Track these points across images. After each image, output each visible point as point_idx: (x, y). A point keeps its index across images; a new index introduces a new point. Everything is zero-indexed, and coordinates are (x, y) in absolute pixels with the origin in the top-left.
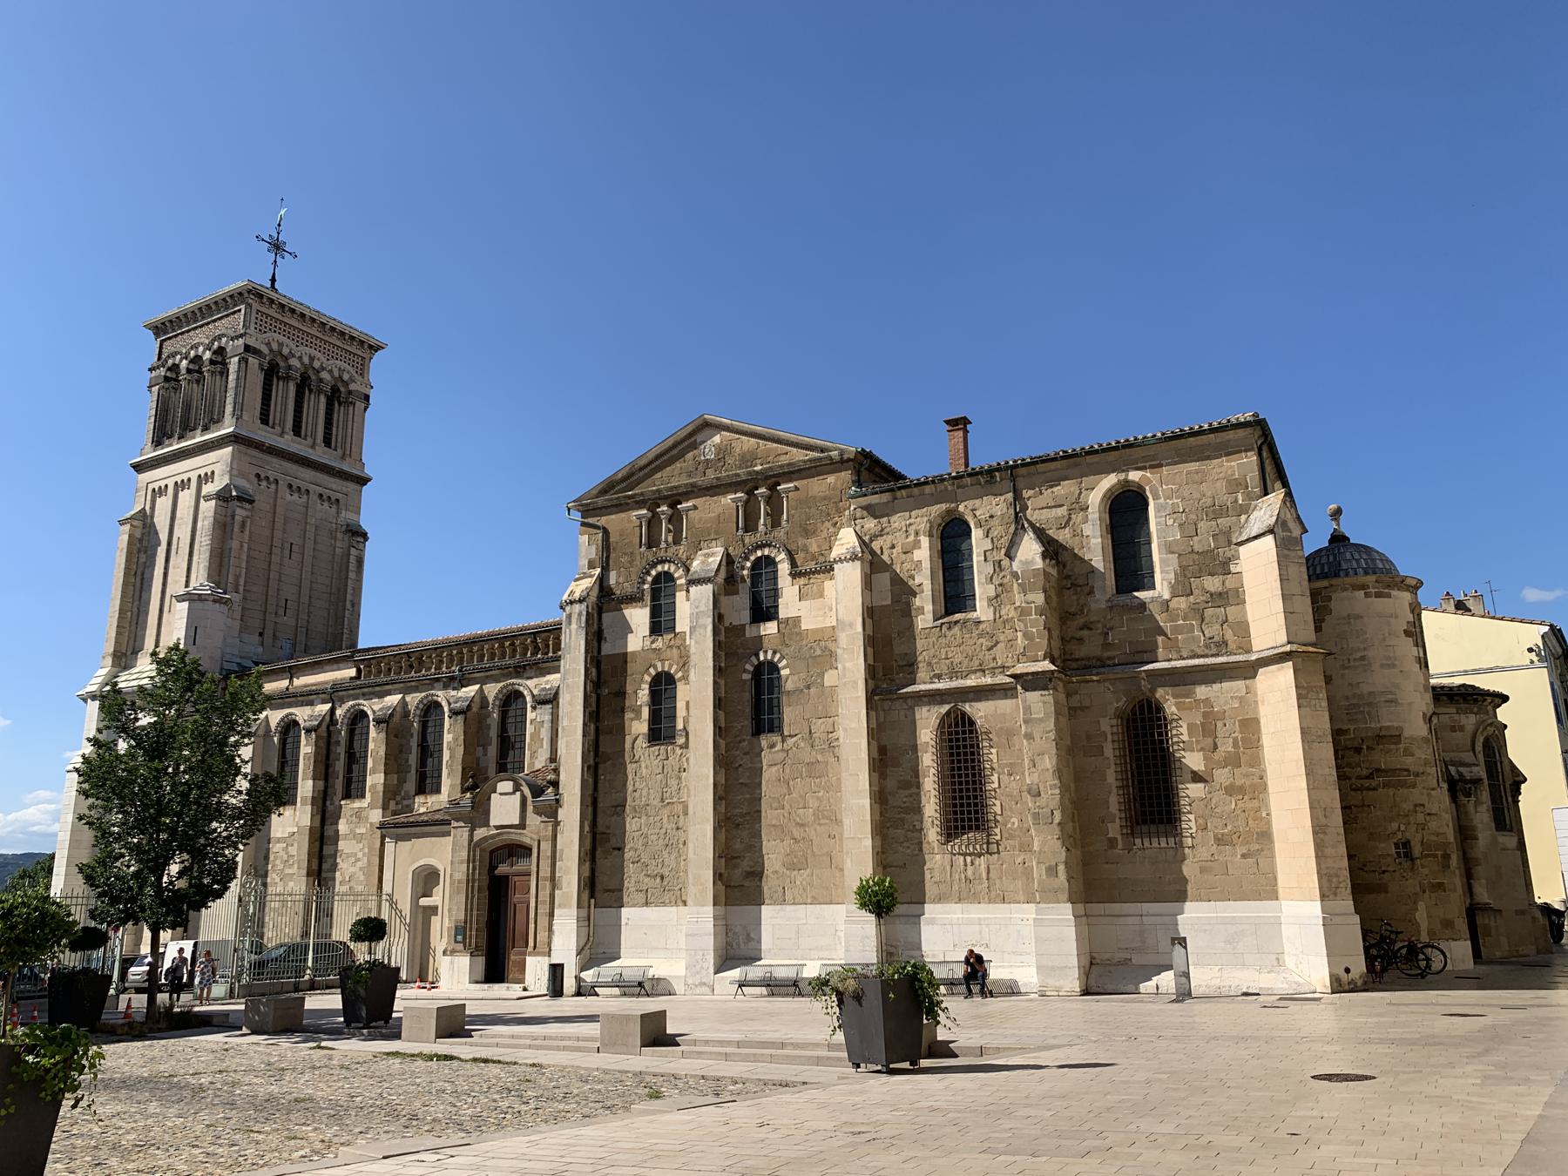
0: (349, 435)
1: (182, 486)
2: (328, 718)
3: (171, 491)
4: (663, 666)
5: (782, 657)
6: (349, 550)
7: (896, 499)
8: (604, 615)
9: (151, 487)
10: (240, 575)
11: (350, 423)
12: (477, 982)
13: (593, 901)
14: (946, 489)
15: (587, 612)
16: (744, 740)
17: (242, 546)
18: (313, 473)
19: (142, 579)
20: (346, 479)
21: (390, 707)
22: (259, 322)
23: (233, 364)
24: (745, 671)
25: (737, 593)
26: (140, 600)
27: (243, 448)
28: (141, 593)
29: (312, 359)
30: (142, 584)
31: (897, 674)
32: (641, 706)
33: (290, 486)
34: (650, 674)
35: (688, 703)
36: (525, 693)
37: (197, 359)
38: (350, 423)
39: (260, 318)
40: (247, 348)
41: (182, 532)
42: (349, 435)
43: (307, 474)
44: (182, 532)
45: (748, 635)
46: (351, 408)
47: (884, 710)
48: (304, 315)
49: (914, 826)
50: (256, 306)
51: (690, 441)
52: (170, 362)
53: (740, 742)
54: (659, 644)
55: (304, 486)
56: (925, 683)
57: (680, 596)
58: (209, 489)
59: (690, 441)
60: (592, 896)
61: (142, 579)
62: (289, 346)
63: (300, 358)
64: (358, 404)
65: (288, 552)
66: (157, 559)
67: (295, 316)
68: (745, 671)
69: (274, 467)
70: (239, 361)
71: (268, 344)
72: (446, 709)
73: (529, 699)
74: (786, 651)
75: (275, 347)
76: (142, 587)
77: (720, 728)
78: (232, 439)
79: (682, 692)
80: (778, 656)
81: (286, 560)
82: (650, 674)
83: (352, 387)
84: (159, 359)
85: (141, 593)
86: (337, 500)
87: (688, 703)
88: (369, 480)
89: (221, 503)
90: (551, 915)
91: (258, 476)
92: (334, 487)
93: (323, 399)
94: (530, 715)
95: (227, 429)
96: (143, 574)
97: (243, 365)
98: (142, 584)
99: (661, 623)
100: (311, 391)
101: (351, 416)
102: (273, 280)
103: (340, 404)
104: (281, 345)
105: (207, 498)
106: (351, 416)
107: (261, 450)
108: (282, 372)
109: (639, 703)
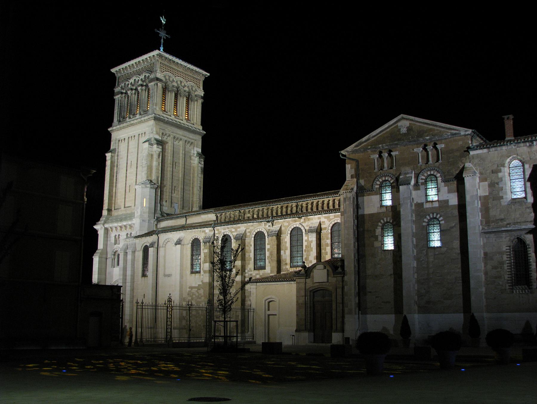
0: (195, 114)
2: (213, 238)
4: (387, 219)
5: (440, 216)
6: (198, 165)
7: (490, 151)
8: (359, 198)
10: (159, 176)
11: (196, 109)
12: (311, 342)
13: (360, 312)
14: (512, 148)
15: (353, 197)
16: (424, 250)
17: (159, 164)
18: (183, 131)
21: (241, 234)
22: (161, 68)
24: (424, 222)
25: (419, 189)
26: (116, 187)
27: (157, 122)
28: (116, 184)
29: (181, 82)
31: (492, 223)
32: (378, 235)
34: (381, 223)
36: (302, 228)
38: (196, 109)
39: (161, 65)
42: (195, 114)
43: (180, 132)
44: (132, 158)
45: (425, 207)
46: (196, 102)
47: (486, 238)
48: (178, 63)
49: (499, 283)
51: (395, 125)
53: (422, 251)
56: (504, 227)
59: (395, 125)
60: (359, 310)
62: (173, 77)
63: (177, 82)
64: (199, 100)
66: (106, 168)
67: (175, 64)
68: (424, 222)
69: (169, 129)
71: (165, 77)
72: (266, 235)
73: (304, 231)
74: (442, 214)
75: (167, 78)
77: (414, 244)
80: (439, 216)
82: (381, 223)
85: (116, 184)
90: (343, 317)
91: (163, 134)
92: (191, 137)
93: (185, 99)
94: (305, 238)
100: (180, 96)
101: (196, 106)
103: (191, 101)
104: (170, 77)
106: (196, 106)
107: (164, 122)
108: (170, 89)
109: (376, 235)
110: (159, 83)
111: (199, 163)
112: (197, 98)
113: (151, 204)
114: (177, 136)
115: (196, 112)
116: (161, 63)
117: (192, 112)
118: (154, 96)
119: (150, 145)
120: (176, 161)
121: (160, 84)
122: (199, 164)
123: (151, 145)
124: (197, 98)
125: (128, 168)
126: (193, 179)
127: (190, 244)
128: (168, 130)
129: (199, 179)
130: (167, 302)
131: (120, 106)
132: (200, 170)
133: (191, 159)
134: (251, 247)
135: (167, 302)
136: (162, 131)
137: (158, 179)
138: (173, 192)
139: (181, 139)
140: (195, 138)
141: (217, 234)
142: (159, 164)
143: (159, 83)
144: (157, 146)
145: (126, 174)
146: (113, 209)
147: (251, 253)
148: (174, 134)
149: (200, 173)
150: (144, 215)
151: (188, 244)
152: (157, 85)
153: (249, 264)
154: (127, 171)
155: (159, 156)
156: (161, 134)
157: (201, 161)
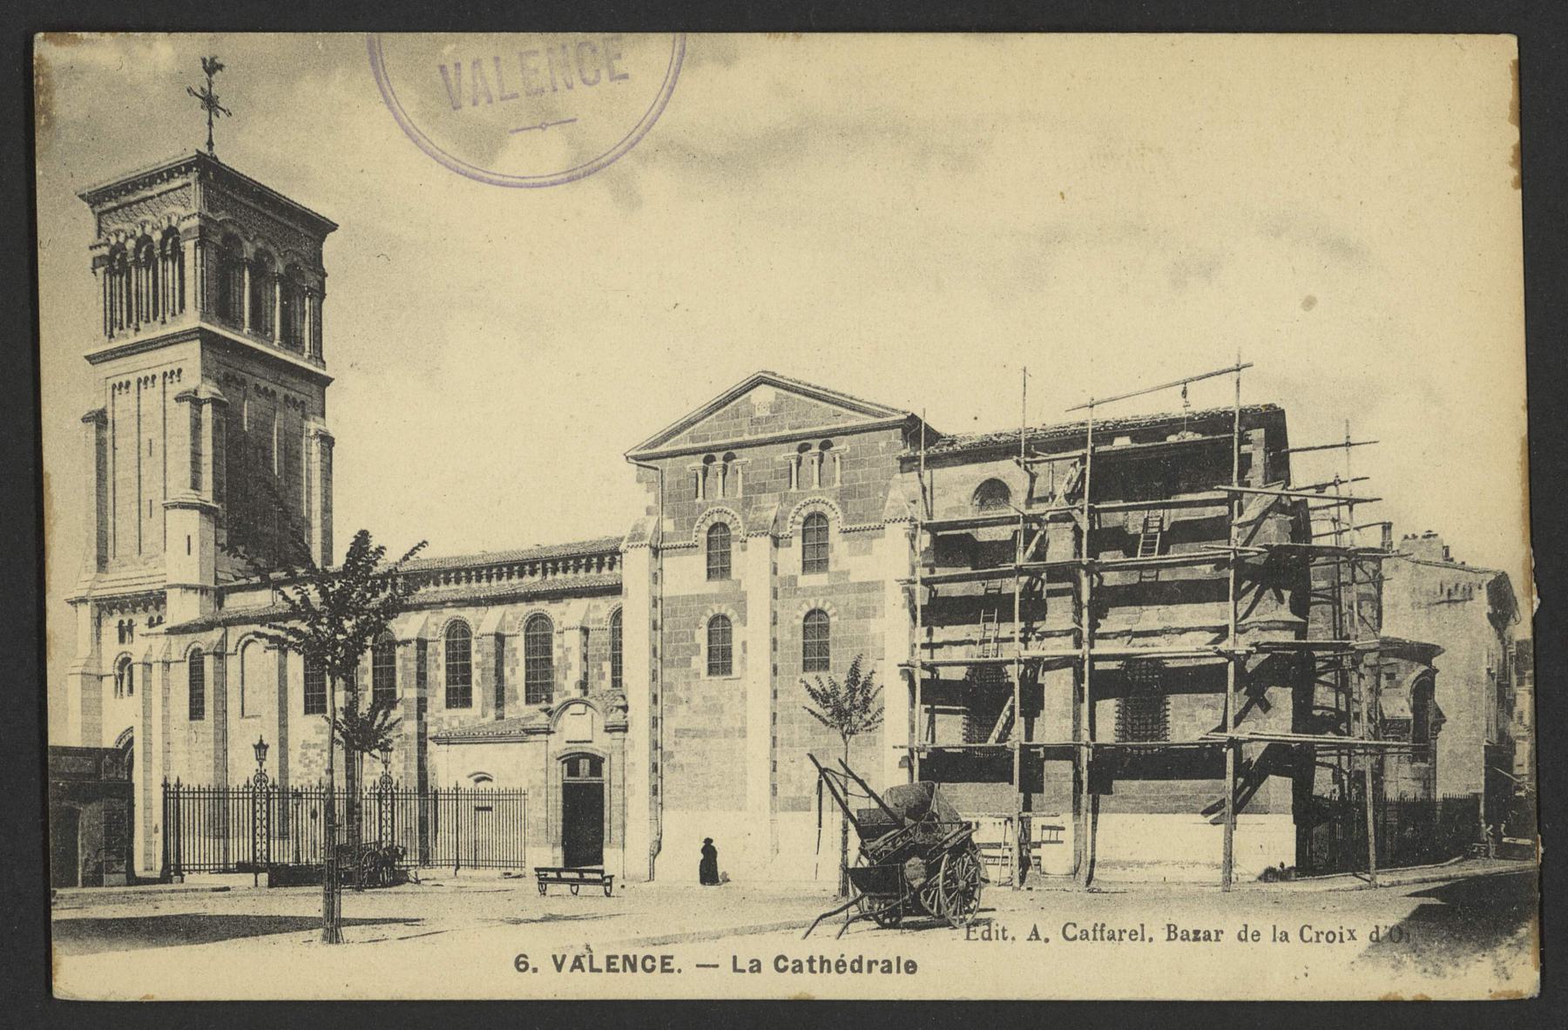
1: (144, 382)
3: (133, 386)
9: (111, 382)
23: (189, 246)
35: (744, 644)
37: (146, 239)
41: (151, 432)
52: (113, 241)
54: (714, 587)
57: (735, 546)
58: (175, 389)
79: (738, 635)
84: (99, 236)
86: (303, 402)
87: (744, 644)
88: (332, 380)
95: (191, 319)
99: (719, 567)
102: (210, 144)
105: (179, 399)
114: (263, 384)
130: (252, 783)
135: (252, 783)
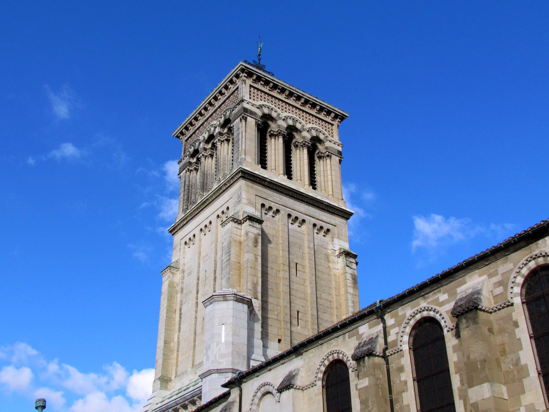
6: (345, 269)
10: (257, 283)
17: (256, 259)
19: (181, 314)
20: (333, 213)
26: (179, 331)
27: (250, 184)
28: (180, 324)
30: (180, 318)
33: (289, 216)
38: (329, 171)
40: (245, 110)
46: (328, 160)
50: (249, 82)
55: (301, 217)
61: (181, 314)
64: (333, 156)
65: (293, 271)
70: (241, 120)
76: (180, 321)
78: (240, 175)
81: (293, 277)
83: (327, 144)
85: (180, 324)
89: (236, 225)
91: (263, 205)
92: (325, 219)
93: (306, 151)
96: (181, 310)
97: (244, 122)
98: (180, 318)
101: (329, 166)
110: (248, 118)
111: (347, 266)
112: (329, 152)
113: (238, 336)
114: (294, 214)
115: (329, 177)
116: (251, 86)
117: (322, 177)
118: (242, 138)
119: (235, 222)
120: (296, 261)
121: (253, 119)
122: (347, 267)
123: (239, 224)
124: (329, 152)
125: (200, 287)
126: (336, 299)
127: (319, 383)
128: (273, 199)
129: (351, 296)
131: (189, 186)
132: (351, 279)
133: (329, 261)
134: (517, 330)
136: (260, 201)
137: (256, 289)
138: (295, 322)
139: (304, 221)
140: (333, 222)
141: (393, 326)
142: (256, 259)
143: (248, 118)
144: (250, 223)
145: (197, 299)
146: (173, 377)
147: (521, 349)
148: (288, 209)
149: (351, 285)
150: (220, 360)
151: (313, 385)
152: (246, 120)
153: (523, 392)
154: (197, 292)
155: (256, 241)
156: (259, 207)
157: (351, 262)
